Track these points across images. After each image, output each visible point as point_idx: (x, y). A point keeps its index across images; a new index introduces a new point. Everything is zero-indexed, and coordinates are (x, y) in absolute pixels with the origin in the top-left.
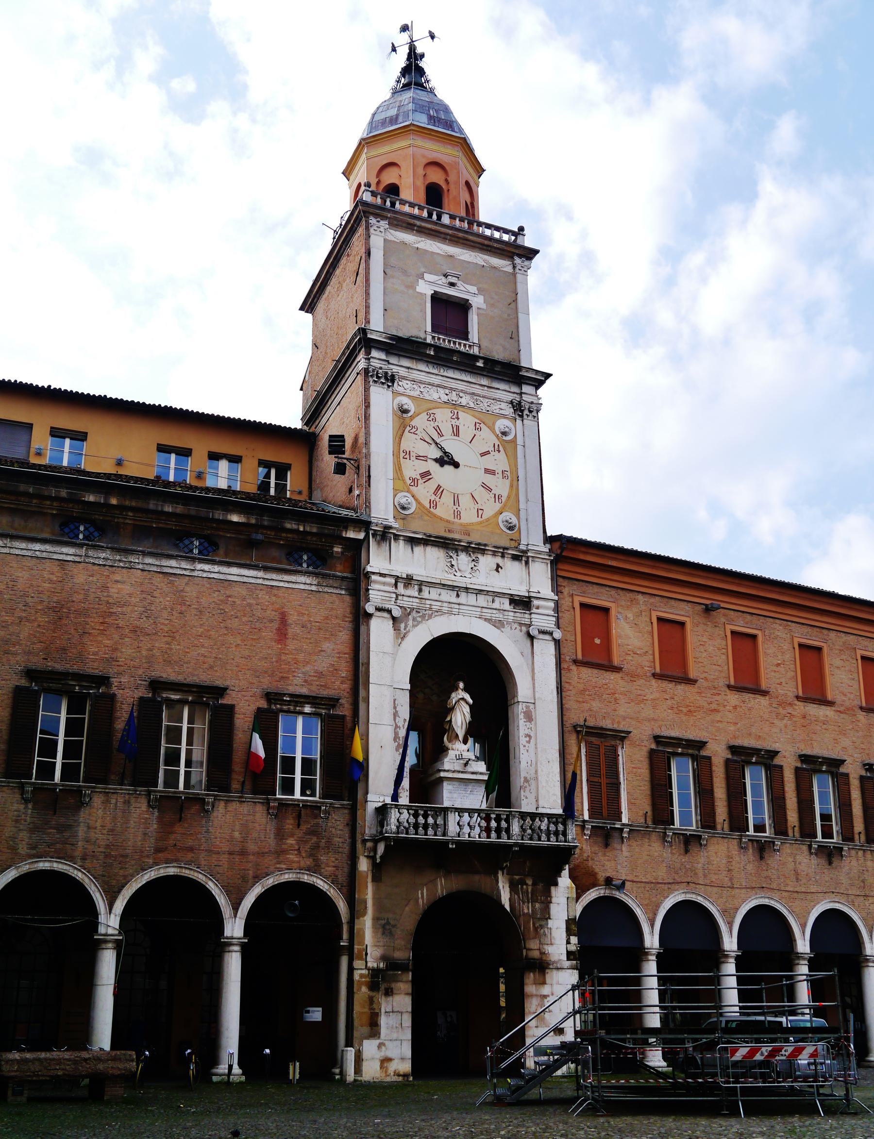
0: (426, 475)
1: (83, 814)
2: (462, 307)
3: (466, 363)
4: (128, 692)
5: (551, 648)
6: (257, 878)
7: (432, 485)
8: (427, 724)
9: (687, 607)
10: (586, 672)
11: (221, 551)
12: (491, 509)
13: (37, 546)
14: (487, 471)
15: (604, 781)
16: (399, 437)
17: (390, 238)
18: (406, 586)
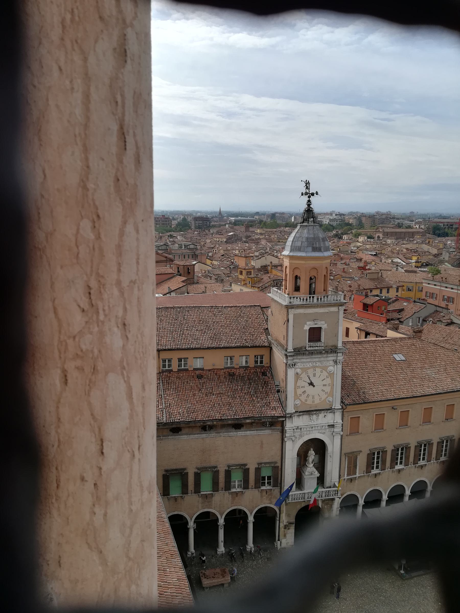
1: (213, 498)
2: (320, 328)
3: (320, 352)
5: (340, 437)
6: (256, 507)
7: (306, 395)
11: (245, 427)
12: (324, 396)
13: (196, 435)
14: (324, 385)
16: (296, 382)
17: (296, 313)
18: (297, 429)
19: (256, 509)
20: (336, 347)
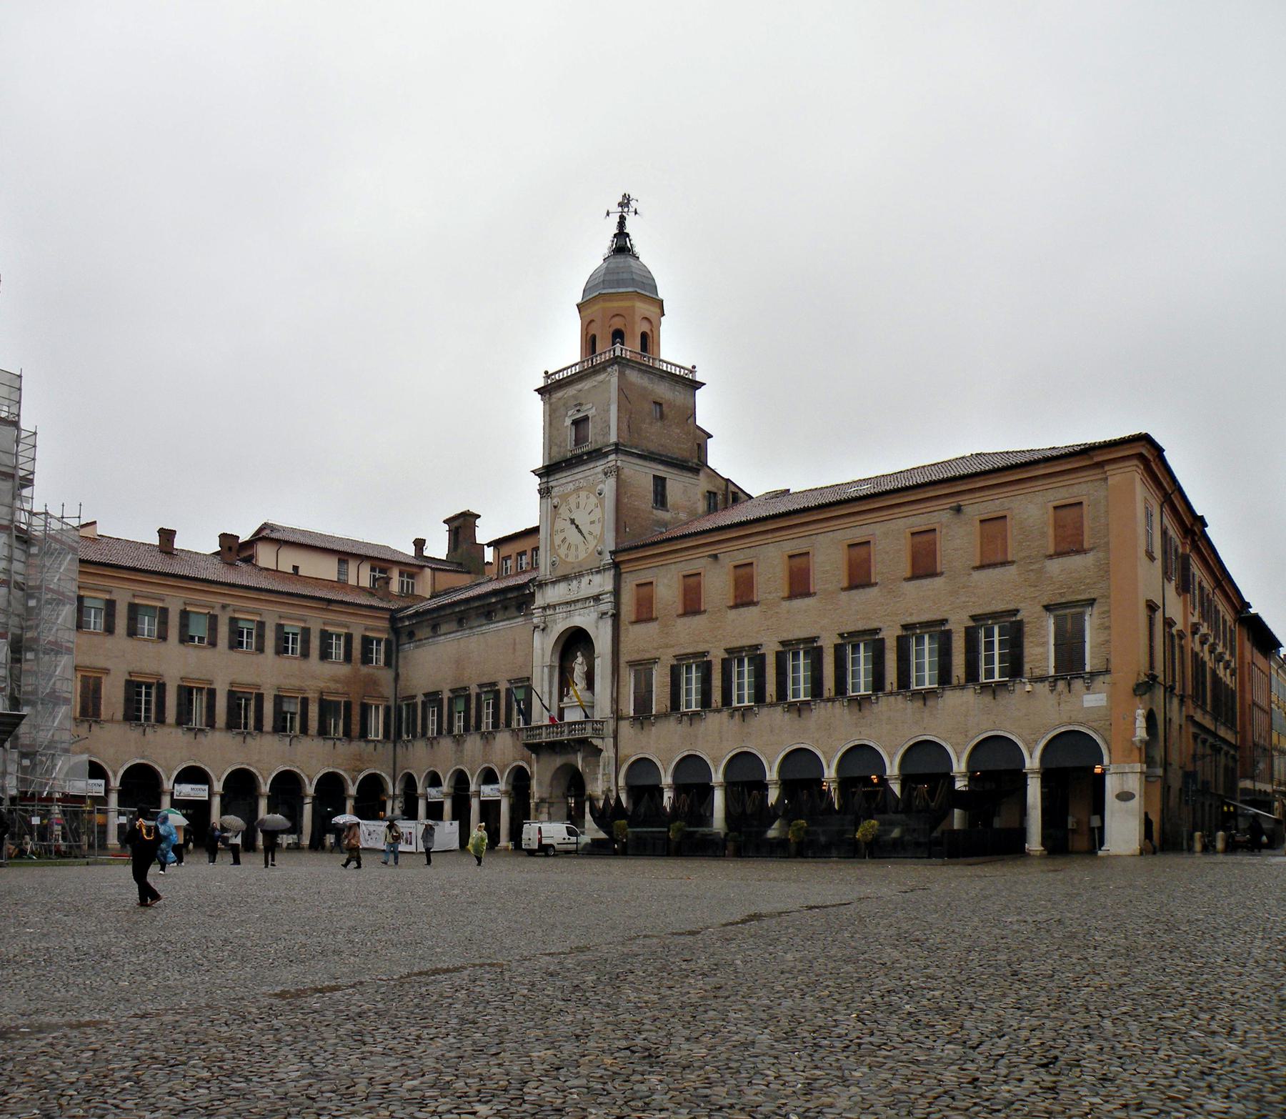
0: (564, 540)
4: (474, 690)
5: (609, 622)
8: (565, 681)
9: (703, 561)
10: (638, 627)
14: (592, 523)
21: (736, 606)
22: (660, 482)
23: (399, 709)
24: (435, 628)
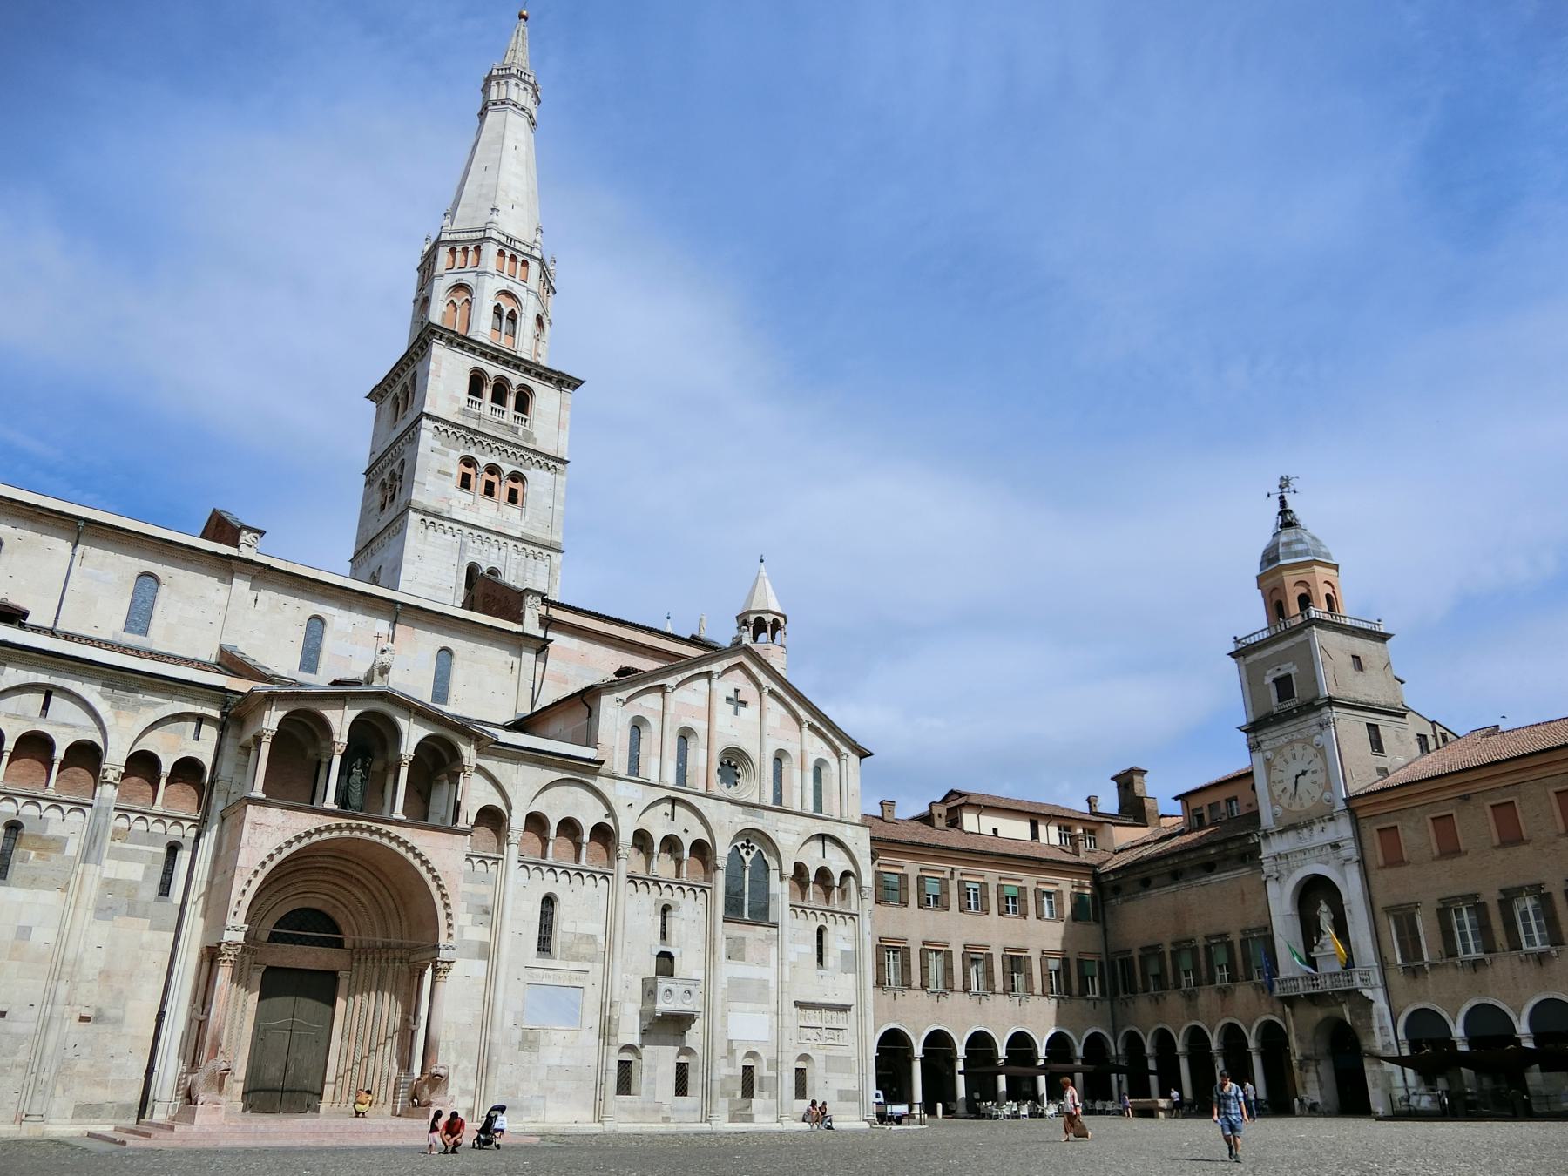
4: (1201, 943)
8: (1310, 931)
10: (1388, 872)
15: (1408, 937)
19: (1255, 1026)
20: (1317, 698)
21: (1504, 844)
22: (1373, 729)
23: (1112, 965)
24: (1146, 883)
